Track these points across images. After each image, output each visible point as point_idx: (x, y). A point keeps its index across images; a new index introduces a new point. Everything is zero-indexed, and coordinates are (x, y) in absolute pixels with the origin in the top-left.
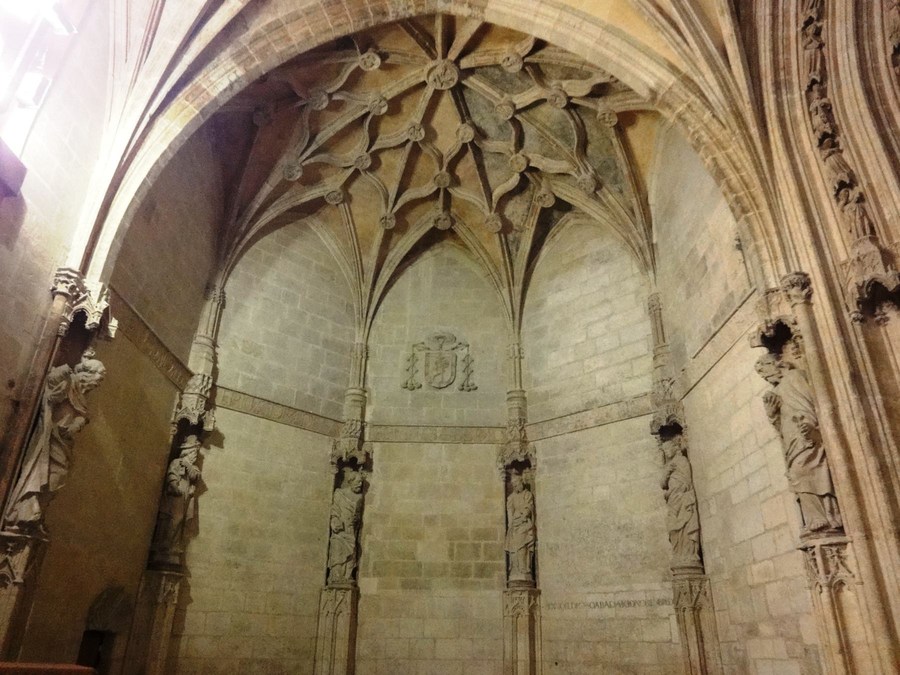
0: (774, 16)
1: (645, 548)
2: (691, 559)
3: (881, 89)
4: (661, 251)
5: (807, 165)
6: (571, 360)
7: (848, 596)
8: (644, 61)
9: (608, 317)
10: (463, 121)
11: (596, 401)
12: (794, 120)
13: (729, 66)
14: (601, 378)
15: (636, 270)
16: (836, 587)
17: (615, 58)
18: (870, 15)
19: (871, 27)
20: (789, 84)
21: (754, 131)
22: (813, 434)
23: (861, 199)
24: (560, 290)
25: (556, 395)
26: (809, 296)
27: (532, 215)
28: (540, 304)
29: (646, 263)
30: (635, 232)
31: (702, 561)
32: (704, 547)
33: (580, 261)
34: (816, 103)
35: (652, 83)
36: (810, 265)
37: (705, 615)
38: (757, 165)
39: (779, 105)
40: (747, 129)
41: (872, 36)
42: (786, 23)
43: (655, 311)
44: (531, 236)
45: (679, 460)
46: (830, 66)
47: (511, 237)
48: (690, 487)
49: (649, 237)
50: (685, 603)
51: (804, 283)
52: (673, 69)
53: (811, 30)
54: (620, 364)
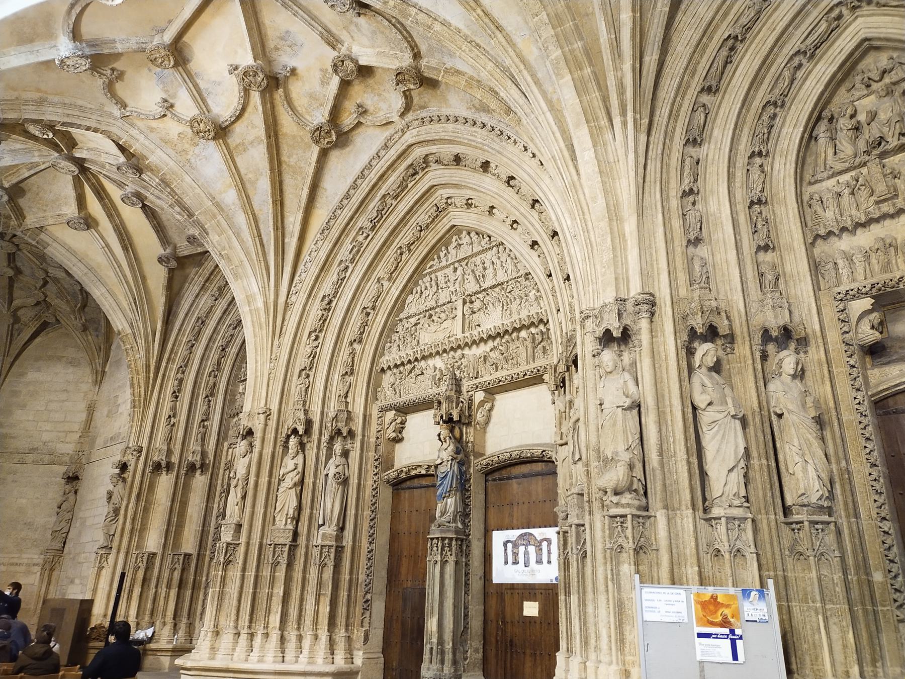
0: (180, 330)
1: (36, 536)
2: (59, 545)
3: (201, 383)
4: (106, 379)
5: (164, 400)
6: (31, 418)
7: (104, 572)
8: (121, 315)
9: (64, 401)
10: (9, 265)
11: (37, 449)
12: (169, 377)
13: (154, 341)
14: (45, 437)
15: (90, 380)
16: (101, 568)
17: (107, 306)
18: (211, 351)
19: (209, 356)
20: (174, 360)
21: (152, 375)
22: (116, 511)
23: (173, 425)
24: (39, 371)
25: (11, 437)
26: (140, 456)
27: (37, 320)
28: (23, 374)
29: (96, 381)
30: (97, 361)
31: (64, 547)
32: (67, 540)
33: (59, 359)
34: (179, 375)
35: (120, 328)
36: (145, 445)
37: (55, 573)
38: (146, 391)
39: (166, 367)
40: (149, 373)
41: (207, 361)
42: (184, 335)
43: (91, 410)
44: (32, 332)
45: (72, 494)
46: (190, 363)
47: (16, 326)
48: (72, 510)
49: (104, 365)
50: (47, 567)
51: (140, 451)
52: (131, 325)
53: (190, 344)
54: (60, 432)
